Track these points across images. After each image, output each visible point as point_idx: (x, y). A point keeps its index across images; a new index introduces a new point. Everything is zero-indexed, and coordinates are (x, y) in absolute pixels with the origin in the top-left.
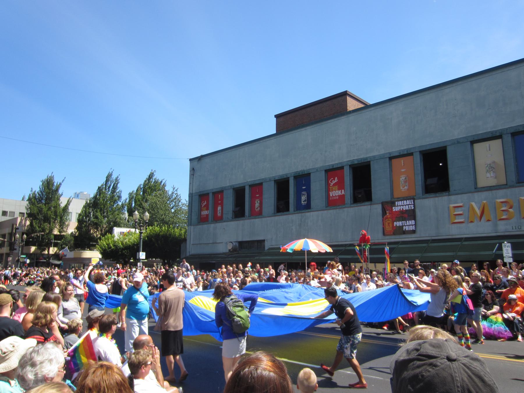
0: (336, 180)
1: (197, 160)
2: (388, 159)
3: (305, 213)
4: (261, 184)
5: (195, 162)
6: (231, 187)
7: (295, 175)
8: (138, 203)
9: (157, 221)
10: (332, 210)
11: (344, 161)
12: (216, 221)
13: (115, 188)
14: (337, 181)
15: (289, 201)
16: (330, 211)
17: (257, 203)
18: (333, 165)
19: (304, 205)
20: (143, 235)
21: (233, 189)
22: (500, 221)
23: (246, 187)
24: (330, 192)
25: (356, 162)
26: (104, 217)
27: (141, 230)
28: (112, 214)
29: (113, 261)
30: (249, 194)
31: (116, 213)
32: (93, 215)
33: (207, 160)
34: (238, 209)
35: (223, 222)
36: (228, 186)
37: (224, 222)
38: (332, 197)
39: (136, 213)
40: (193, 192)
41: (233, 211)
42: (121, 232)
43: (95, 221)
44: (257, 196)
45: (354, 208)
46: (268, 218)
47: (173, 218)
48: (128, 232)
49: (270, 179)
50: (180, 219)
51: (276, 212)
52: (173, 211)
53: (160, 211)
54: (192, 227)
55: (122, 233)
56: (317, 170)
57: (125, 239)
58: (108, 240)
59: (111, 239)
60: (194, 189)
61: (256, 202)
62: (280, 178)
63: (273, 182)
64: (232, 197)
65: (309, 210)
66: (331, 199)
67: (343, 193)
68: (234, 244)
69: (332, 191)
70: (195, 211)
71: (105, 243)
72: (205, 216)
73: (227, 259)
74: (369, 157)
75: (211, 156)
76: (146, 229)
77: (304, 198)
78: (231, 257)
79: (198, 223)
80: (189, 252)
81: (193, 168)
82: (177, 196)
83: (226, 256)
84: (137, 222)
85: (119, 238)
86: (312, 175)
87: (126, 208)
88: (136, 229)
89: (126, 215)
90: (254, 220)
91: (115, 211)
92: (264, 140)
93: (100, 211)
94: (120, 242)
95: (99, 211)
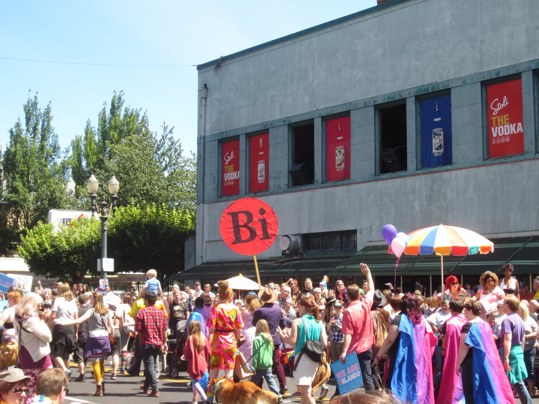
1: (214, 67)
3: (440, 174)
5: (210, 72)
6: (284, 121)
7: (419, 94)
8: (95, 159)
9: (135, 196)
10: (495, 166)
11: (522, 62)
12: (255, 193)
13: (46, 130)
14: (507, 104)
15: (405, 149)
16: (492, 168)
17: (339, 154)
18: (498, 71)
19: (439, 157)
20: (107, 223)
21: (289, 125)
23: (315, 120)
24: (493, 129)
26: (31, 190)
27: (103, 213)
28: (44, 183)
29: (51, 276)
30: (322, 135)
31: (52, 181)
32: (8, 187)
33: (233, 67)
34: (299, 166)
35: (269, 195)
36: (279, 120)
37: (272, 194)
39: (93, 178)
40: (206, 135)
41: (291, 173)
42: (64, 219)
43: (13, 199)
46: (361, 185)
47: (167, 189)
48: (79, 219)
49: (365, 104)
50: (181, 191)
51: (378, 171)
52: (166, 174)
53: (139, 174)
54: (206, 206)
55: (65, 221)
57: (74, 233)
58: (41, 235)
59: (47, 233)
60: (208, 127)
61: (337, 152)
62: (387, 101)
63: (373, 107)
64: (287, 143)
65: (449, 167)
66: (494, 142)
67: (520, 129)
68: (293, 239)
69: (497, 125)
70: (211, 174)
71: (34, 242)
72: (233, 183)
73: (279, 271)
75: (242, 58)
76: (114, 211)
77: (437, 141)
78: (287, 267)
79: (218, 197)
80: (202, 257)
81: (206, 85)
82: (172, 144)
83: (277, 265)
84: (94, 197)
85: (61, 231)
86: (453, 93)
87: (70, 171)
88: (93, 212)
89: (71, 185)
90: (333, 189)
91: (50, 176)
92: (352, 22)
93: (22, 177)
94: (63, 239)
95: (20, 178)
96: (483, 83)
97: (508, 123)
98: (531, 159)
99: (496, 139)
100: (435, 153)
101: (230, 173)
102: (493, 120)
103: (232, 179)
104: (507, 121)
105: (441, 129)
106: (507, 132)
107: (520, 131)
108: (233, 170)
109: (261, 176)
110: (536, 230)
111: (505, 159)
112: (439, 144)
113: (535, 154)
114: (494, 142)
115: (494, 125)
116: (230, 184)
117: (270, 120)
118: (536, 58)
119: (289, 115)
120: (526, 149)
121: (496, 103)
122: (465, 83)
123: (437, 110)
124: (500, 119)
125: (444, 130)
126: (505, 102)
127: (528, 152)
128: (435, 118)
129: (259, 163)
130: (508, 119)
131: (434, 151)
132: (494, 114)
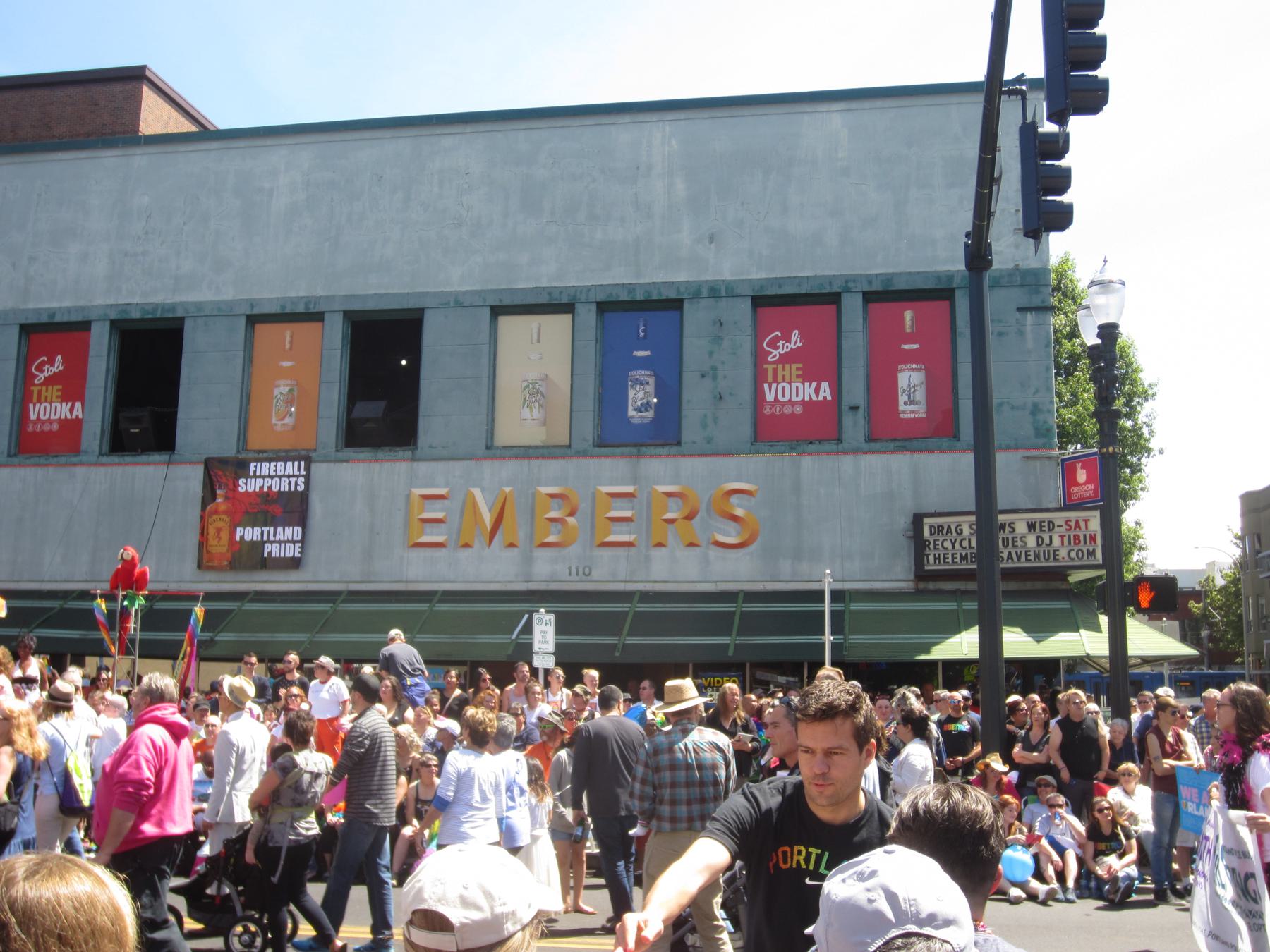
0: (796, 341)
2: (243, 321)
4: (675, 305)
7: (756, 294)
10: (28, 469)
14: (799, 344)
16: (22, 472)
18: (889, 278)
22: (602, 549)
24: (766, 386)
25: (136, 315)
38: (773, 404)
45: (109, 469)
51: (106, 448)
56: (715, 292)
66: (767, 411)
67: (826, 392)
69: (775, 380)
74: (182, 304)
97: (801, 380)
98: (89, 465)
99: (773, 406)
100: (633, 417)
101: (48, 406)
102: (766, 370)
103: (53, 417)
104: (798, 376)
105: (652, 373)
106: (797, 396)
107: (825, 398)
108: (57, 397)
109: (912, 402)
110: (892, 581)
111: (46, 460)
112: (644, 401)
113: (98, 457)
114: (768, 410)
115: (770, 378)
116: (46, 428)
117: (827, 273)
118: (119, 303)
120: (83, 447)
121: (776, 339)
122: (459, 305)
123: (642, 335)
124: (784, 369)
125: (656, 376)
126: (796, 341)
127: (86, 452)
129: (902, 370)
130: (800, 372)
131: (631, 413)
132: (769, 359)
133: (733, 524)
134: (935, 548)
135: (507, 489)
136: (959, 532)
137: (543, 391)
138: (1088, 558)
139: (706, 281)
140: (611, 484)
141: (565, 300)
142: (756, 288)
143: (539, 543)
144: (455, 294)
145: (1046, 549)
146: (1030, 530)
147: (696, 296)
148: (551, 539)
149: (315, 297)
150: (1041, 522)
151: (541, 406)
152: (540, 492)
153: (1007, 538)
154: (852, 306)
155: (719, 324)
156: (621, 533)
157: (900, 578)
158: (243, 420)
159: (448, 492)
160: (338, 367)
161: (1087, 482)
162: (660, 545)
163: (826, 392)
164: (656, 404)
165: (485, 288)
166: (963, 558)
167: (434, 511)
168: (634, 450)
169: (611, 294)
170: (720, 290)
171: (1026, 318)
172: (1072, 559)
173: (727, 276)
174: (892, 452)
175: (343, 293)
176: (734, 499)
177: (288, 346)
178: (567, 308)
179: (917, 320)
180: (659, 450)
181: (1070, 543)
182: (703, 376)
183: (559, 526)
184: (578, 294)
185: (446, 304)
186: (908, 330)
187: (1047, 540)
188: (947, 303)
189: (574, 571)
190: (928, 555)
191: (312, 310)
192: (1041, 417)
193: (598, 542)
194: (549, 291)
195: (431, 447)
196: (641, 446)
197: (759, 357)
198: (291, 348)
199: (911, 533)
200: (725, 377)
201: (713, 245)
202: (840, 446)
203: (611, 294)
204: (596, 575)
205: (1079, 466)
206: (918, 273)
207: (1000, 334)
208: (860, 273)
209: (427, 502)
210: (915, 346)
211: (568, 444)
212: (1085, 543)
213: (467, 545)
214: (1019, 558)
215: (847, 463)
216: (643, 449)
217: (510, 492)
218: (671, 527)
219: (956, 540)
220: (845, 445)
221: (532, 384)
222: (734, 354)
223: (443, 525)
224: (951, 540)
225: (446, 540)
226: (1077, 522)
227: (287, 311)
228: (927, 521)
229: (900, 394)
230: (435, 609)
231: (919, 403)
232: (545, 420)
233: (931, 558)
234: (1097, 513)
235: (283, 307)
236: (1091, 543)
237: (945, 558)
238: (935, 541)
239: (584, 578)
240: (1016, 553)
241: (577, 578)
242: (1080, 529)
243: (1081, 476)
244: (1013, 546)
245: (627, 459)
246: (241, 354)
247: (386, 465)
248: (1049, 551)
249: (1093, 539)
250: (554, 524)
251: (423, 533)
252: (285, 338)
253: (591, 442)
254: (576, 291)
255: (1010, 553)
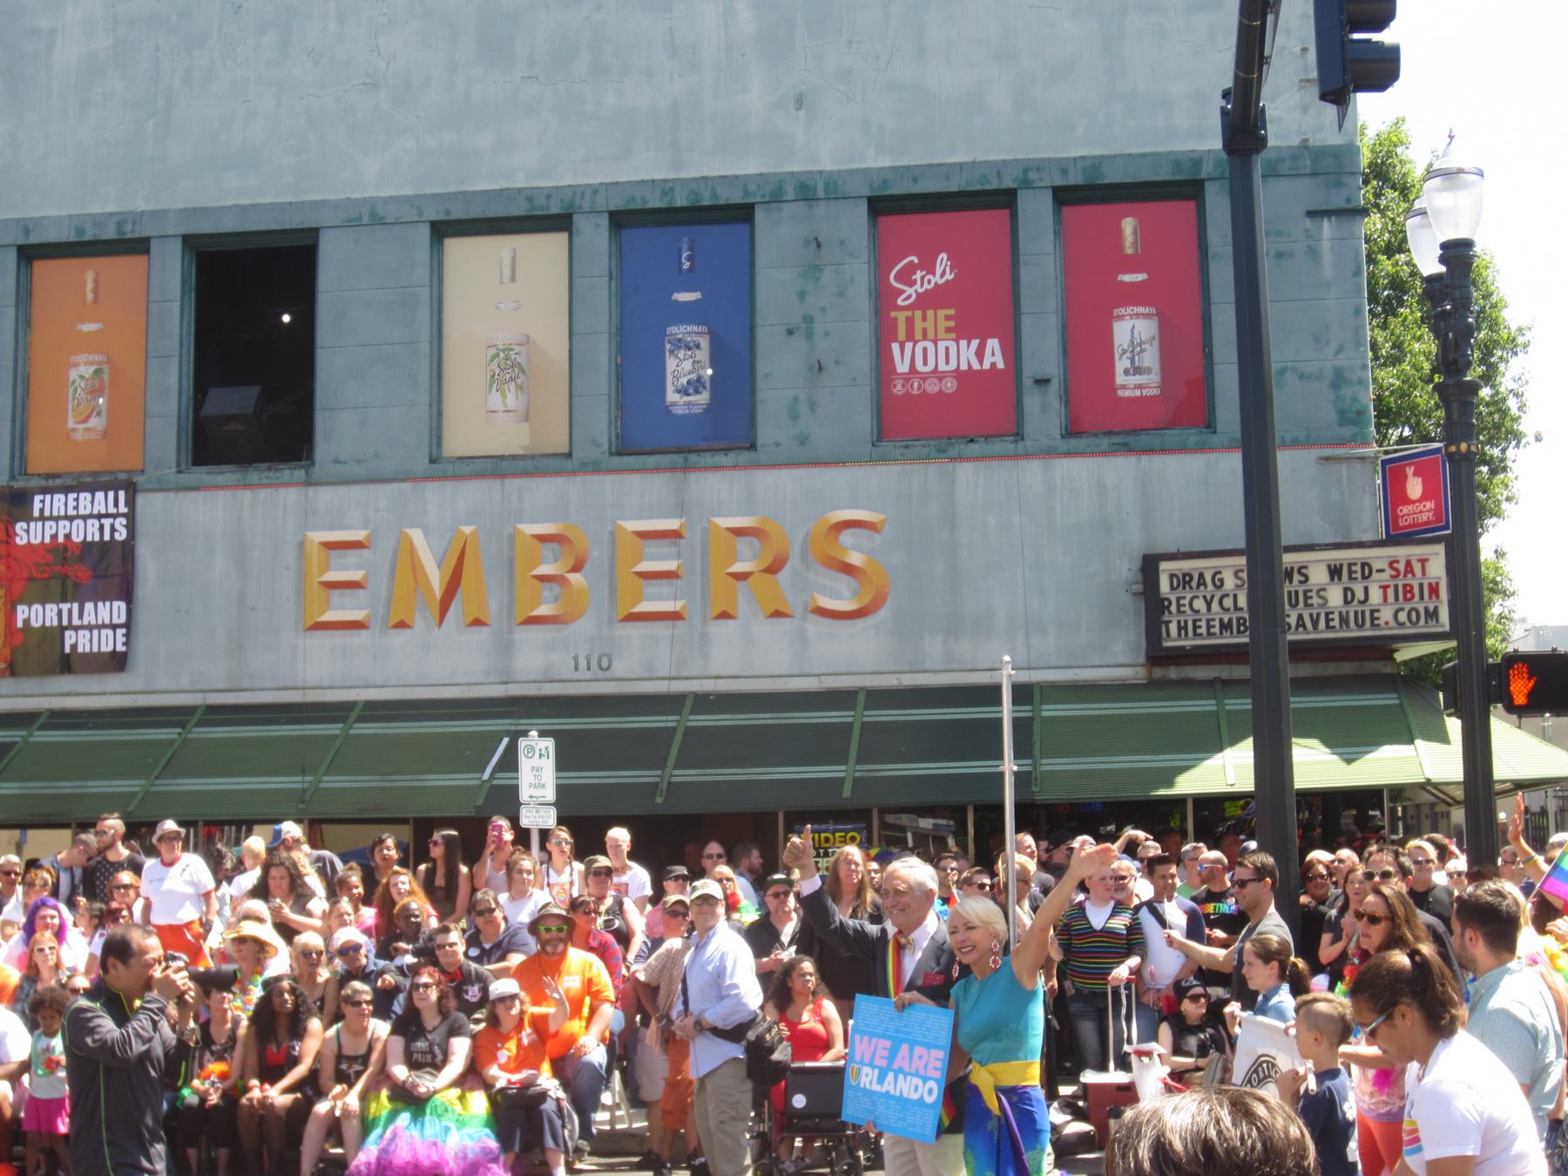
0: (944, 270)
2: (12, 255)
4: (742, 214)
7: (875, 194)
14: (949, 276)
18: (1095, 163)
24: (895, 347)
44: (88, 327)
69: (910, 336)
96: (872, 202)
97: (953, 335)
99: (907, 380)
100: (674, 404)
104: (948, 330)
106: (947, 362)
107: (993, 365)
109: (1137, 370)
110: (1109, 666)
112: (693, 376)
114: (899, 387)
117: (993, 157)
119: (353, 196)
121: (911, 268)
122: (377, 220)
123: (686, 265)
124: (924, 319)
126: (944, 270)
128: (679, 290)
129: (1121, 317)
130: (952, 324)
131: (672, 396)
133: (845, 578)
134: (1179, 611)
135: (467, 530)
136: (1218, 583)
137: (522, 363)
138: (1426, 622)
139: (792, 174)
140: (640, 517)
141: (555, 209)
142: (876, 184)
143: (521, 619)
144: (372, 203)
145: (1360, 609)
146: (1332, 579)
147: (776, 198)
148: (543, 610)
149: (134, 214)
150: (1350, 565)
151: (520, 388)
152: (522, 533)
153: (1297, 593)
154: (1036, 210)
155: (814, 245)
156: (660, 598)
157: (1123, 660)
158: (18, 425)
159: (368, 537)
160: (176, 331)
161: (1421, 500)
162: (725, 615)
163: (994, 354)
164: (712, 378)
165: (419, 192)
166: (1225, 626)
167: (346, 568)
168: (678, 459)
169: (633, 198)
170: (815, 190)
171: (1321, 227)
172: (1404, 624)
173: (827, 164)
174: (1105, 454)
175: (181, 206)
176: (847, 537)
177: (90, 296)
178: (560, 222)
179: (1143, 232)
180: (720, 459)
181: (1397, 598)
182: (790, 332)
183: (556, 589)
184: (578, 201)
185: (354, 220)
186: (1129, 251)
187: (1360, 595)
188: (1192, 204)
189: (583, 663)
190: (1167, 623)
191: (129, 236)
192: (1347, 392)
193: (622, 613)
194: (529, 195)
195: (337, 461)
196: (690, 451)
197: (883, 298)
198: (95, 301)
199: (1139, 588)
200: (827, 334)
201: (801, 113)
202: (1020, 445)
203: (633, 198)
204: (619, 669)
205: (1410, 471)
206: (1144, 155)
207: (1280, 255)
208: (1046, 155)
209: (333, 553)
210: (1140, 277)
211: (566, 450)
212: (1422, 598)
213: (402, 625)
214: (1315, 623)
215: (1032, 472)
216: (693, 457)
217: (472, 532)
218: (741, 584)
219: (1212, 597)
220: (1028, 444)
221: (503, 351)
222: (842, 294)
223: (361, 592)
224: (1205, 597)
225: (368, 616)
226: (1408, 563)
227: (88, 237)
228: (1166, 567)
229: (1117, 356)
230: (352, 732)
231: (1148, 371)
232: (528, 410)
233: (1173, 628)
234: (1440, 549)
235: (80, 231)
236: (1430, 598)
237: (1195, 628)
238: (1178, 599)
239: (601, 674)
240: (1311, 615)
241: (589, 675)
242: (1413, 575)
243: (1414, 487)
244: (1306, 605)
245: (668, 474)
246: (11, 312)
247: (263, 494)
248: (1363, 612)
249: (1434, 590)
250: (547, 585)
251: (327, 606)
252: (85, 282)
253: (606, 447)
254: (574, 193)
255: (1300, 617)
